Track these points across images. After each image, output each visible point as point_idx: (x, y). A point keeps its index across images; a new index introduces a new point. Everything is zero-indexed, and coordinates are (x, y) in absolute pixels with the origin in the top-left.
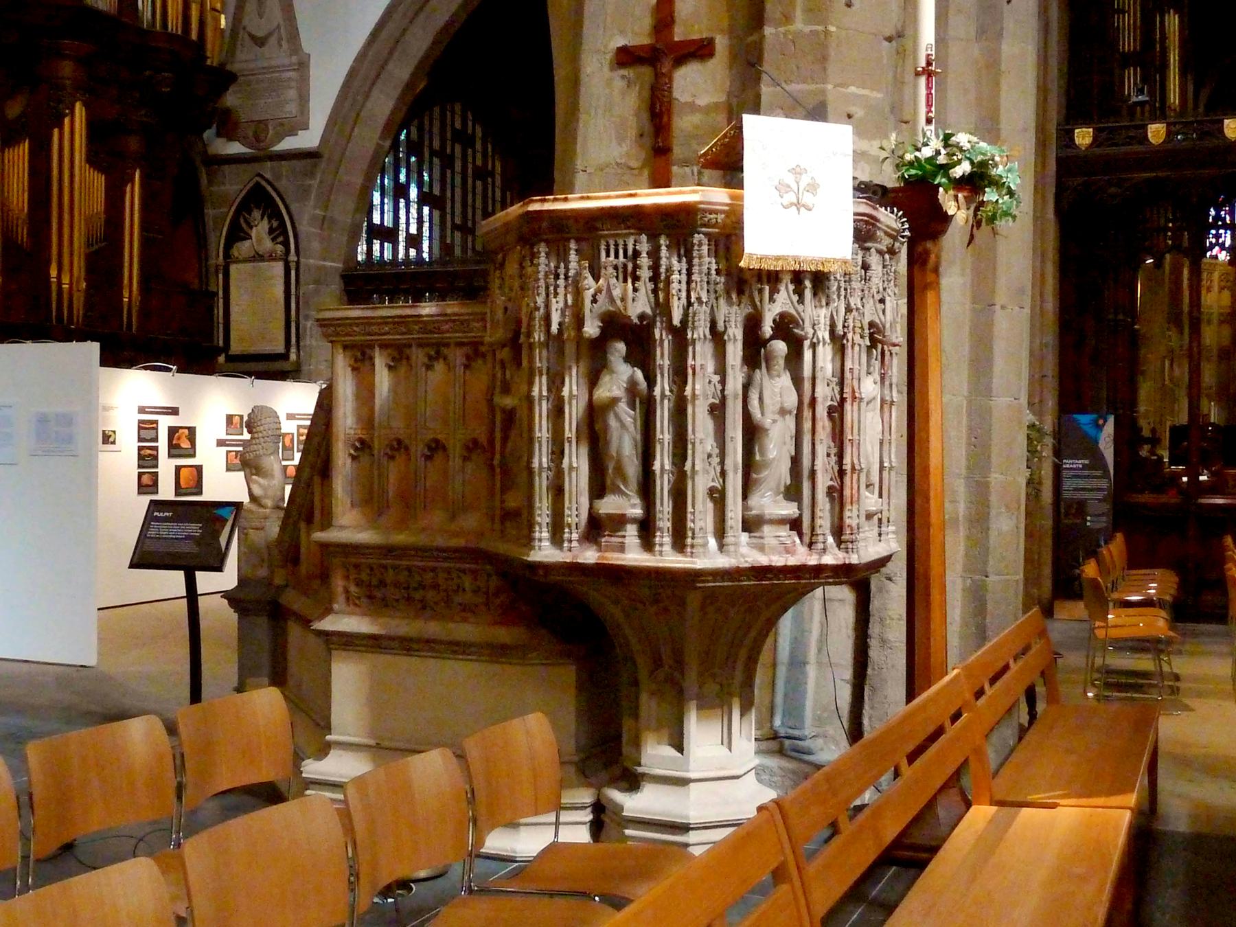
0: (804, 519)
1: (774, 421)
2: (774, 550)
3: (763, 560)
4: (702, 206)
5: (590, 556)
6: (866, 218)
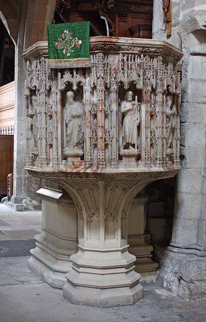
1: (70, 120)
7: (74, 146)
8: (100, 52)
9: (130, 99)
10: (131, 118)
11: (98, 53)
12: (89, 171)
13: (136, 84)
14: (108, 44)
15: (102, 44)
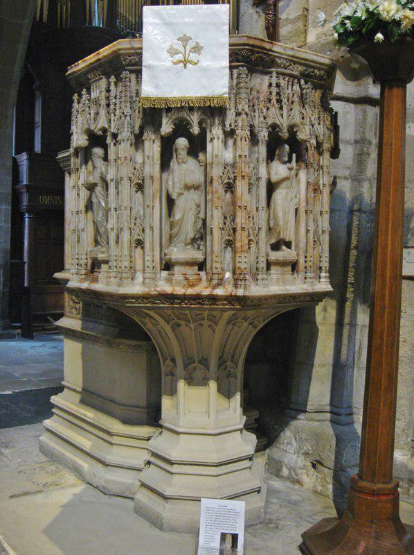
0: (207, 264)
1: (180, 194)
2: (179, 284)
3: (168, 289)
4: (122, 52)
5: (85, 285)
6: (247, 47)
7: (188, 244)
8: (243, 66)
9: (286, 159)
10: (287, 194)
11: (239, 66)
12: (219, 292)
13: (296, 132)
14: (258, 52)
15: (248, 49)
